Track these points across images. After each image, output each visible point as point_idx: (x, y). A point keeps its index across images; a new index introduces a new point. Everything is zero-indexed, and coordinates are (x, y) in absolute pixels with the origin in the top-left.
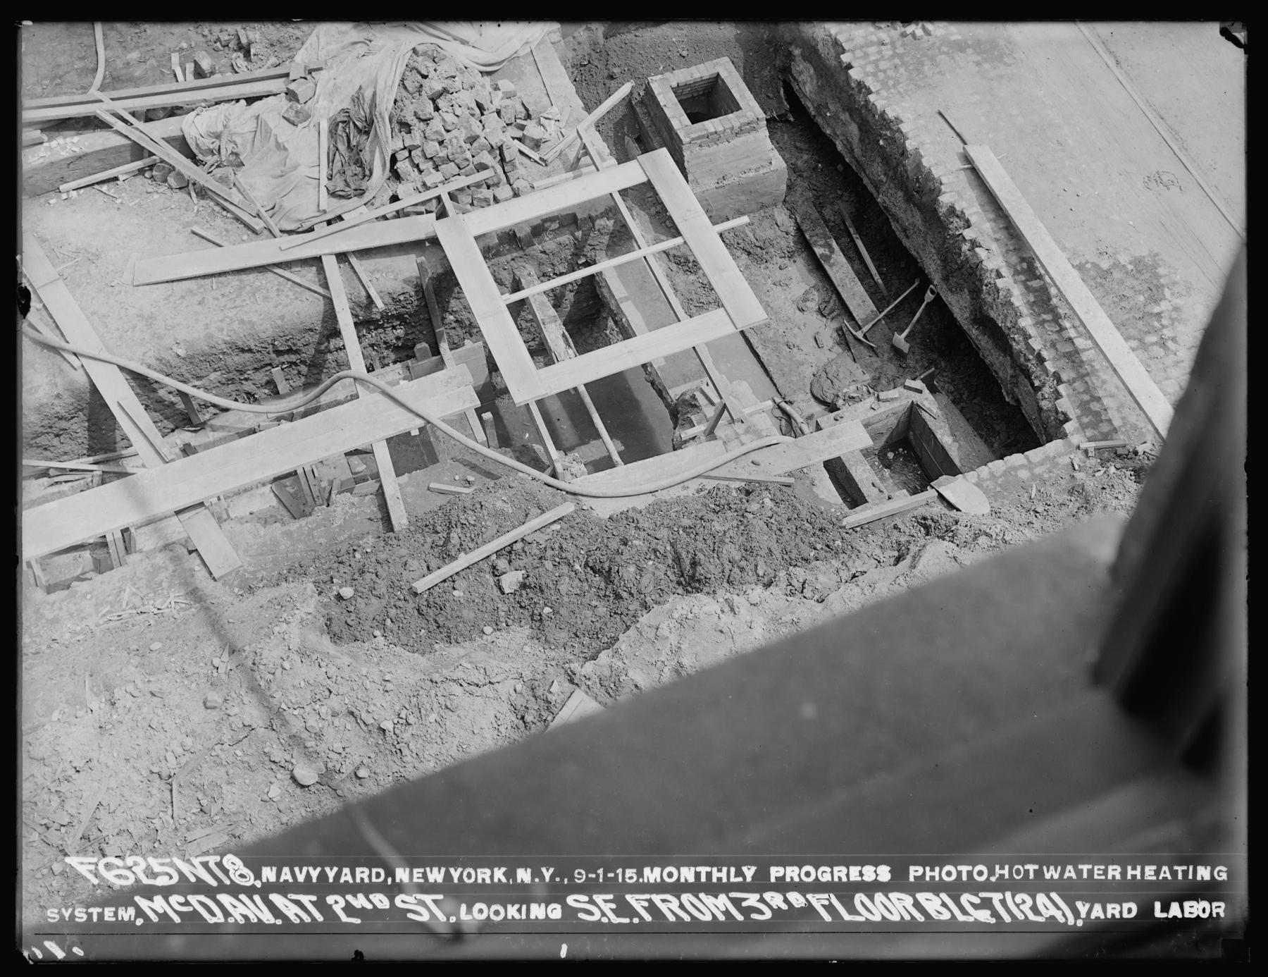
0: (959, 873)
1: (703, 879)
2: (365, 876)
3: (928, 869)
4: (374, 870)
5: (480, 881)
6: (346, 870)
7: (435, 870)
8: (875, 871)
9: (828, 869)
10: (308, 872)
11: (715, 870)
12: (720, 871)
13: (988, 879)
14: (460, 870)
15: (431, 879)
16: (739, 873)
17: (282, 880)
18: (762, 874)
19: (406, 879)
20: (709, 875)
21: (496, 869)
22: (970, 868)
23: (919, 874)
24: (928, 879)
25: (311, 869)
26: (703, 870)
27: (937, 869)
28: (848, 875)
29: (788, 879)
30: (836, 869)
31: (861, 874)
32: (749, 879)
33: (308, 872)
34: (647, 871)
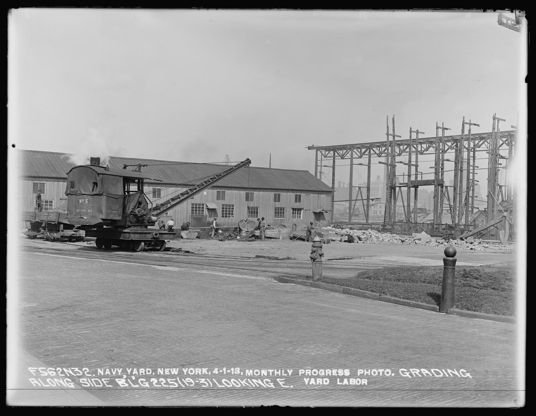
0: (379, 373)
1: (271, 374)
2: (143, 372)
3: (365, 370)
4: (147, 369)
5: (196, 374)
6: (135, 370)
7: (174, 369)
8: (344, 373)
9: (323, 371)
10: (117, 370)
11: (276, 370)
12: (278, 371)
13: (391, 375)
14: (187, 369)
15: (173, 373)
16: (286, 372)
17: (106, 374)
18: (296, 373)
19: (162, 373)
20: (273, 373)
21: (203, 369)
22: (383, 370)
23: (362, 373)
24: (365, 375)
25: (118, 369)
26: (271, 371)
27: (369, 370)
28: (332, 373)
29: (306, 375)
30: (327, 370)
31: (337, 373)
32: (290, 375)
33: (117, 370)
34: (247, 371)
